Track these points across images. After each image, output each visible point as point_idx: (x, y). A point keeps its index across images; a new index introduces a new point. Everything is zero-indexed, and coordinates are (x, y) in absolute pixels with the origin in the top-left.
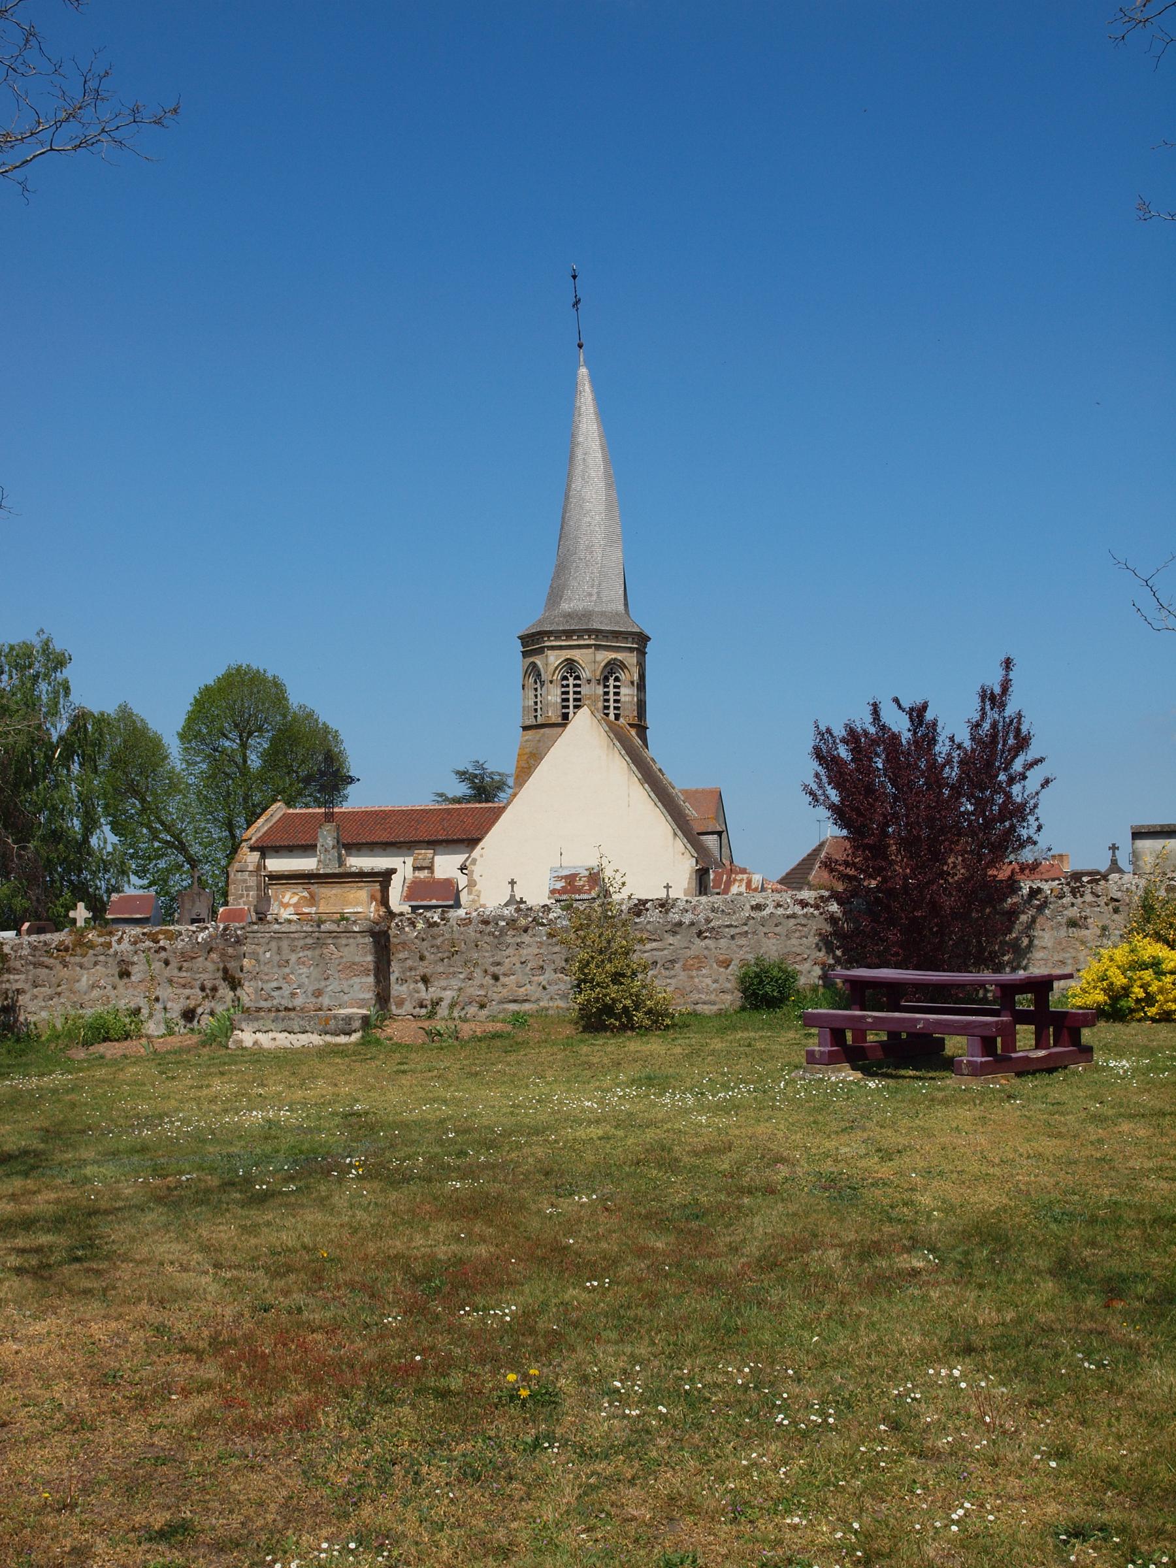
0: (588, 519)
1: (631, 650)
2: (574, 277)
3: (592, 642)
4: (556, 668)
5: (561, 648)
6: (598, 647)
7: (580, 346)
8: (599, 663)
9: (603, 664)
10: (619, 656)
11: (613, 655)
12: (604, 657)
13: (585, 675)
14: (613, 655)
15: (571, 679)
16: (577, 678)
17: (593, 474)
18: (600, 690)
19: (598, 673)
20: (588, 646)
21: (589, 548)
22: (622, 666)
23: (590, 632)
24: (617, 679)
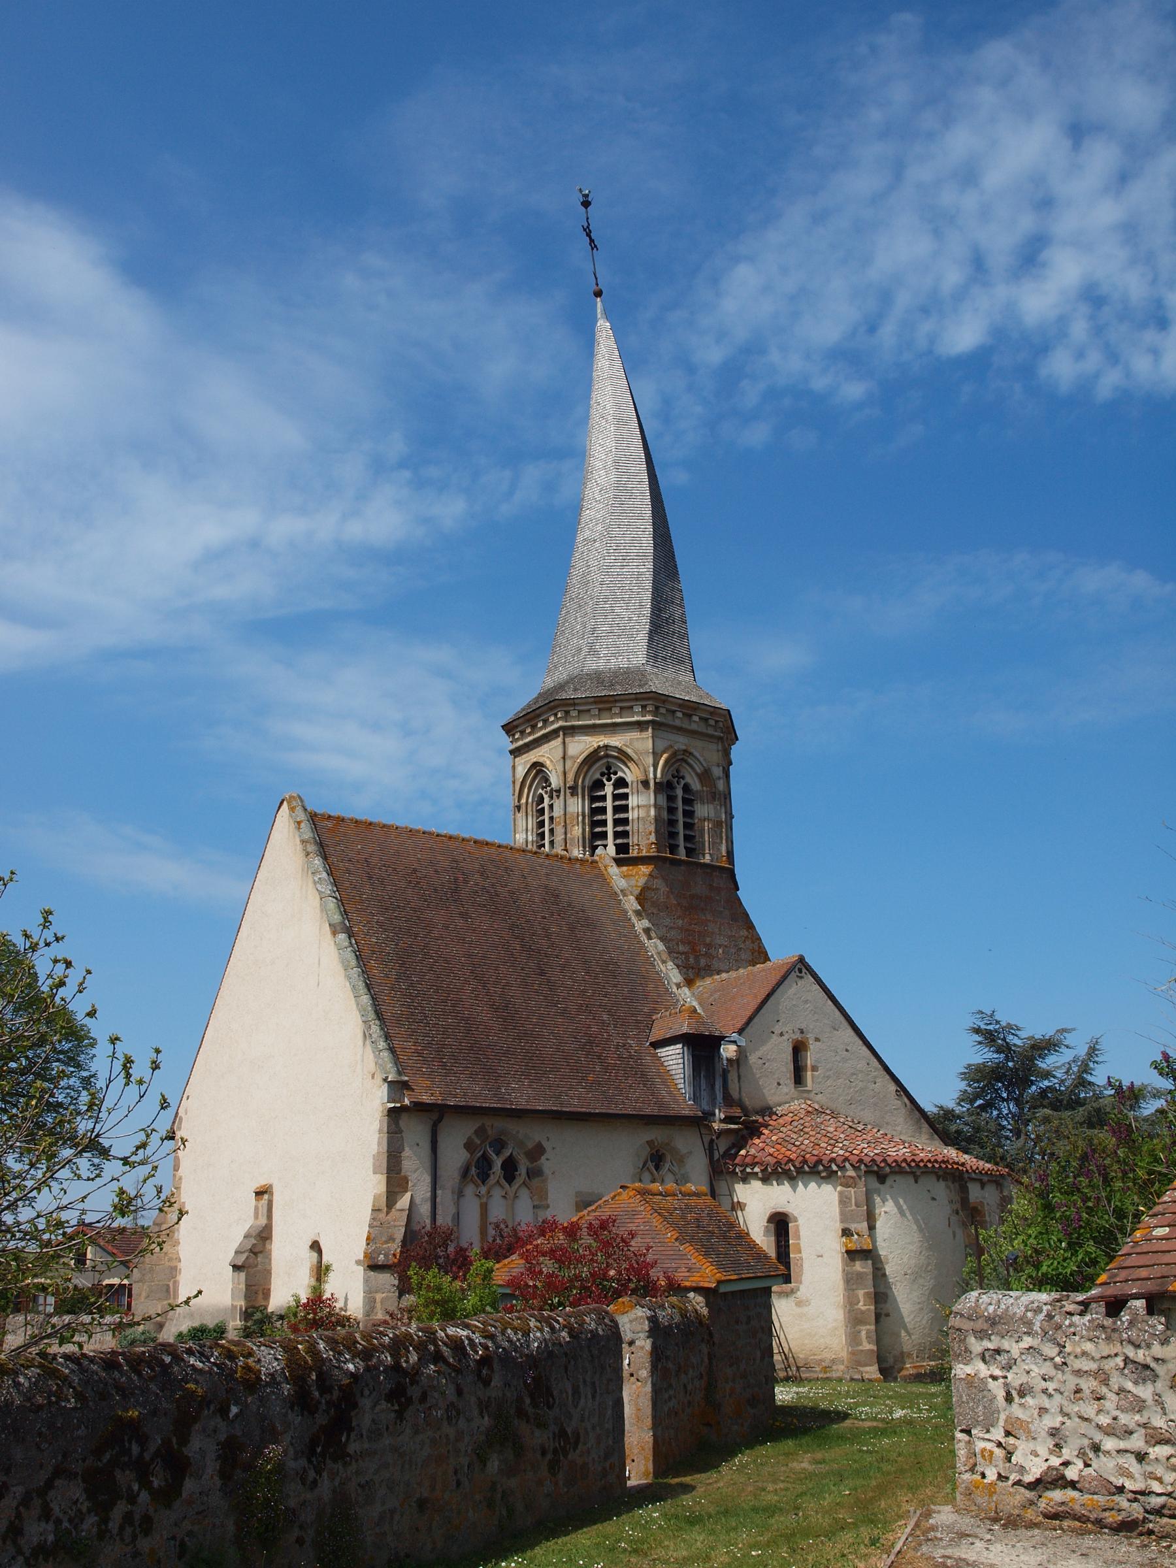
0: (587, 533)
1: (640, 726)
2: (586, 204)
7: (598, 294)
8: (574, 758)
10: (615, 741)
12: (581, 746)
13: (555, 781)
17: (598, 464)
18: (577, 805)
20: (555, 733)
22: (624, 756)
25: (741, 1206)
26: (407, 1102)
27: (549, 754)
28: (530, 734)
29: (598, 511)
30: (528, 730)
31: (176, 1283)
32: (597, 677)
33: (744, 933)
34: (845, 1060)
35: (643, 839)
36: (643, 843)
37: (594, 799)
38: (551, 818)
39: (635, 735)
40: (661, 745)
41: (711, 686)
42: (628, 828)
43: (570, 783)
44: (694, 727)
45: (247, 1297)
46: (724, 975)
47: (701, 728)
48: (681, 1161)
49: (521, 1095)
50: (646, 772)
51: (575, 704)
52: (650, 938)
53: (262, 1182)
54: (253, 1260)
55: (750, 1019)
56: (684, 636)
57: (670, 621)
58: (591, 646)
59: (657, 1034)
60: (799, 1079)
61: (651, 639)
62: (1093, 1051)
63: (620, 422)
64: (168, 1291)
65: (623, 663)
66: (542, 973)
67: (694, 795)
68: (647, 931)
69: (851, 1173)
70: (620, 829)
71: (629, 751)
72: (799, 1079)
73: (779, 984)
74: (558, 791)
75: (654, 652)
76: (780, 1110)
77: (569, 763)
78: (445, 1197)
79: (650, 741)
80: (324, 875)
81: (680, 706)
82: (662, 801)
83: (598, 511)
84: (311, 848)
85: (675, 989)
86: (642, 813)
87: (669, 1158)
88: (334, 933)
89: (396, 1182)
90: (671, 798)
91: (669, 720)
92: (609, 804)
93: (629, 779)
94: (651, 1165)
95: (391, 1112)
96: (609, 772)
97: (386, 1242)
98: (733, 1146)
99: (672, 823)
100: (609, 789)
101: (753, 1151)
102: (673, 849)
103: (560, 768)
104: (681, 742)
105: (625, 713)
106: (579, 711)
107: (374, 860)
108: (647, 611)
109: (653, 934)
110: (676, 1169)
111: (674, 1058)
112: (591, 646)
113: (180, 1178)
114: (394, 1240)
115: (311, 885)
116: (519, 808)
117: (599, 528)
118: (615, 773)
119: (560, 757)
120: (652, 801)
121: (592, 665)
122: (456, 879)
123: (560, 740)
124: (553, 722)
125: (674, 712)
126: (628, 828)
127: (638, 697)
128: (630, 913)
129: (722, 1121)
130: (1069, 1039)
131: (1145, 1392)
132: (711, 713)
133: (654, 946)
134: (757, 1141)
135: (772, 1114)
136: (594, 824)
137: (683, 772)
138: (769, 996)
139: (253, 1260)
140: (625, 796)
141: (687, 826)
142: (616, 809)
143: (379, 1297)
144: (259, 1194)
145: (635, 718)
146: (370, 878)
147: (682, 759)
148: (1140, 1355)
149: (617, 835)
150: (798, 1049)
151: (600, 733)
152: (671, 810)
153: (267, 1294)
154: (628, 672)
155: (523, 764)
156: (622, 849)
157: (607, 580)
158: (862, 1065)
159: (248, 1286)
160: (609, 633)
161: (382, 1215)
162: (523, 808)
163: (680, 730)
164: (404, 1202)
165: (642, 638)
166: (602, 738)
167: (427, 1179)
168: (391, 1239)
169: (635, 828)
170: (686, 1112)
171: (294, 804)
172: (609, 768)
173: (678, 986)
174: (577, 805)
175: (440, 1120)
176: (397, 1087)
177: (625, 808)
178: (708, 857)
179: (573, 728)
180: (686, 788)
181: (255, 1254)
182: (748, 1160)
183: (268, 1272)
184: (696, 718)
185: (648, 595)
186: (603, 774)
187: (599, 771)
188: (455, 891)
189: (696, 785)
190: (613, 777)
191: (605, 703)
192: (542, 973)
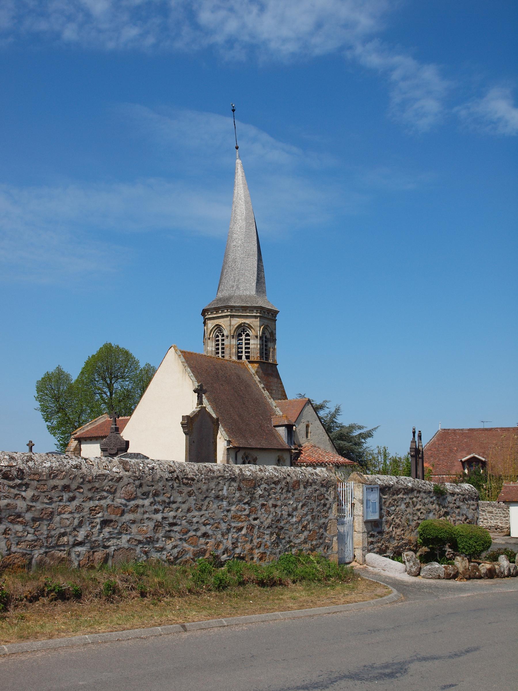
0: (235, 243)
1: (256, 317)
2: (233, 110)
3: (229, 313)
4: (211, 330)
5: (214, 318)
6: (232, 316)
7: (237, 148)
9: (236, 326)
10: (247, 321)
12: (237, 322)
13: (226, 333)
15: (220, 336)
16: (223, 336)
17: (239, 218)
18: (234, 342)
19: (232, 332)
20: (227, 316)
21: (234, 261)
22: (250, 327)
23: (227, 307)
24: (248, 335)
26: (231, 446)
27: (223, 323)
28: (215, 314)
32: (240, 297)
33: (280, 385)
34: (317, 430)
35: (255, 355)
38: (223, 344)
39: (254, 320)
40: (262, 323)
44: (270, 317)
49: (253, 444)
56: (264, 283)
58: (237, 286)
59: (274, 422)
61: (257, 285)
62: (337, 410)
63: (246, 202)
65: (248, 293)
67: (268, 339)
68: (263, 388)
69: (331, 466)
70: (247, 350)
71: (252, 325)
72: (307, 437)
74: (227, 337)
75: (257, 291)
76: (303, 445)
77: (232, 327)
84: (186, 364)
90: (262, 341)
93: (251, 334)
95: (228, 449)
96: (244, 331)
98: (296, 457)
101: (302, 459)
103: (228, 328)
107: (197, 367)
111: (282, 431)
112: (237, 286)
119: (229, 325)
120: (259, 343)
121: (238, 293)
123: (229, 319)
131: (484, 514)
133: (266, 393)
135: (302, 446)
136: (238, 348)
140: (249, 340)
141: (266, 350)
145: (254, 314)
148: (483, 509)
149: (246, 352)
150: (307, 426)
155: (211, 324)
156: (247, 357)
158: (321, 431)
162: (211, 339)
165: (254, 284)
170: (287, 447)
172: (244, 330)
175: (239, 451)
176: (229, 442)
177: (249, 344)
179: (234, 315)
180: (266, 337)
185: (256, 269)
186: (242, 332)
189: (268, 336)
190: (245, 333)
191: (244, 308)
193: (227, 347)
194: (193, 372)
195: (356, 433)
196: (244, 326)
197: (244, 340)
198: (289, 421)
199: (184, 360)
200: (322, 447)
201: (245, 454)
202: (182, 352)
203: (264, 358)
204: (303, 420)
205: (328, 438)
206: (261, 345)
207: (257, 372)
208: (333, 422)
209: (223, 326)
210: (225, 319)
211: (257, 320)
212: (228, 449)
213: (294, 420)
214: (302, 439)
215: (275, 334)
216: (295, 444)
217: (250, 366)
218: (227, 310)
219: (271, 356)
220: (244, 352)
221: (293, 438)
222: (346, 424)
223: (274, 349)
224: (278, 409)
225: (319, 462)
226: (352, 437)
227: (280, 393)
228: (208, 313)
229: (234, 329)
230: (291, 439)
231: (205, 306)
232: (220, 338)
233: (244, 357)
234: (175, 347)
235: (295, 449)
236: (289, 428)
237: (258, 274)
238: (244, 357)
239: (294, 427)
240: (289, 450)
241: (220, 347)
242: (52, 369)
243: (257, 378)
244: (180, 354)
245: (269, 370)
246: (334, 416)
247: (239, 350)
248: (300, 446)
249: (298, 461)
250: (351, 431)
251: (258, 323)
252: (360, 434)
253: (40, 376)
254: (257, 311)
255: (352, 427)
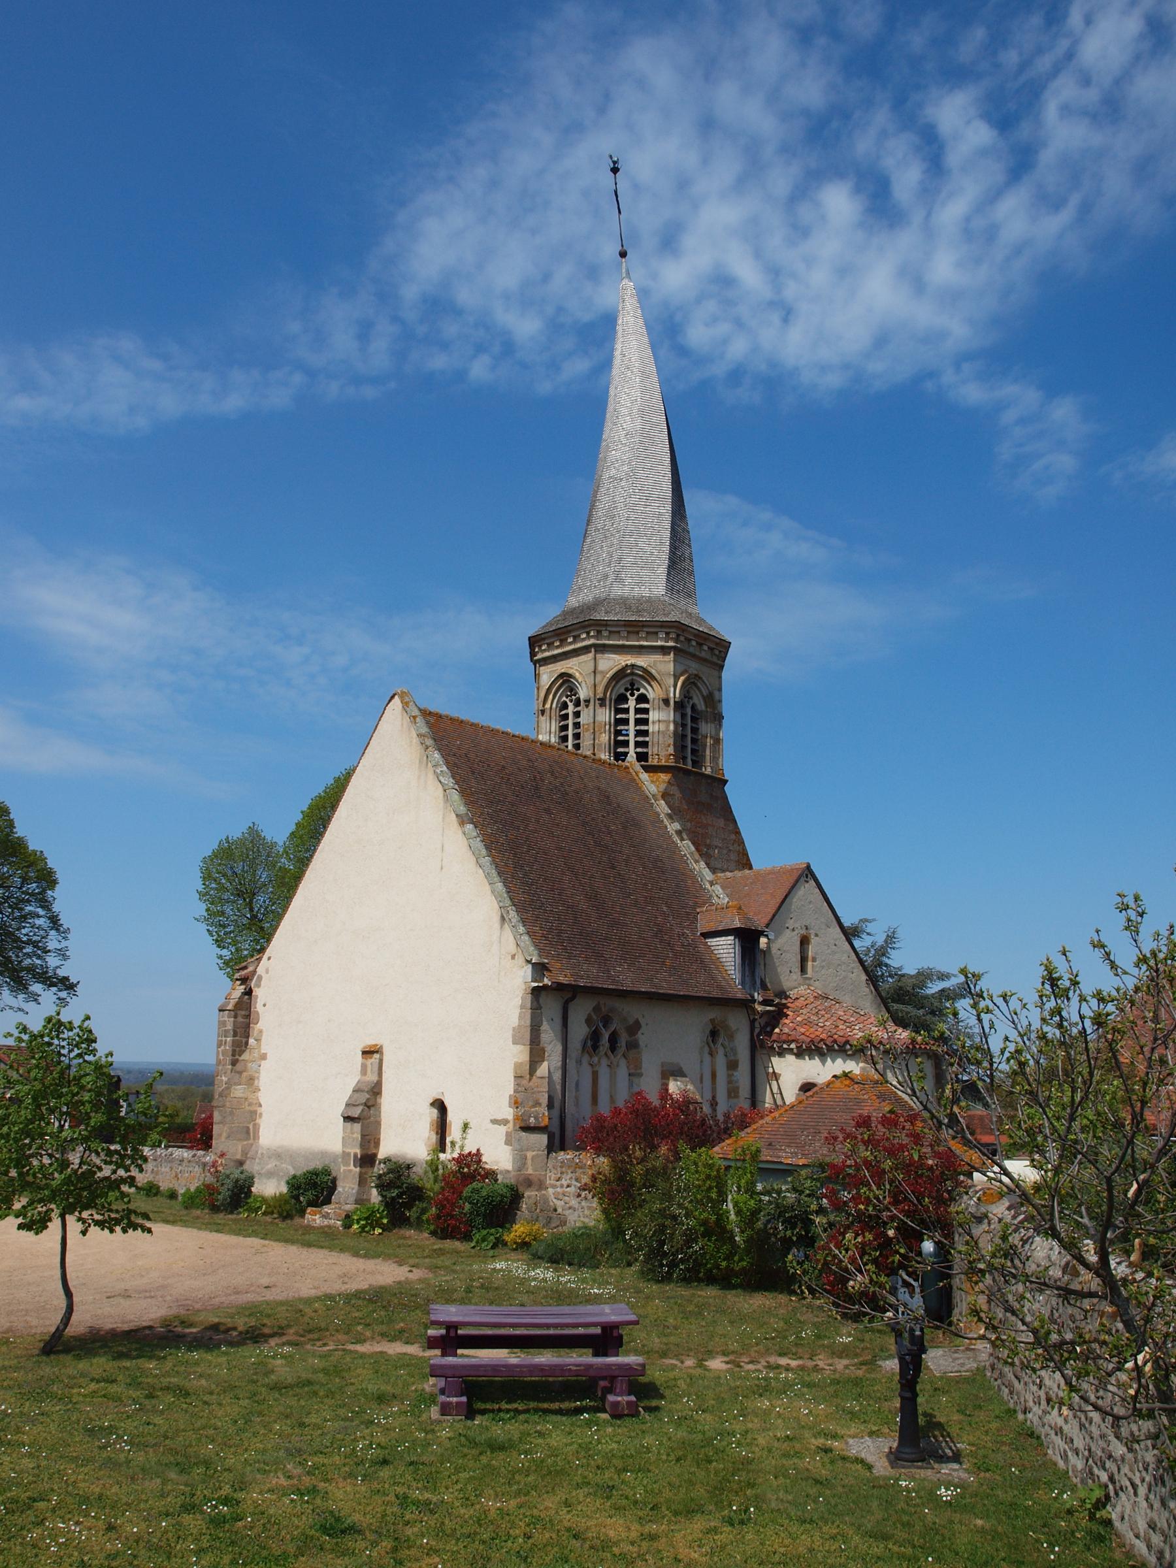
0: (613, 472)
1: (664, 650)
3: (592, 641)
6: (601, 649)
8: (604, 673)
9: (609, 675)
10: (641, 661)
11: (629, 660)
12: (611, 663)
13: (583, 694)
14: (629, 660)
17: (624, 411)
19: (600, 689)
22: (648, 676)
24: (643, 699)
25: (776, 1076)
26: (546, 981)
27: (578, 667)
28: (557, 647)
29: (624, 453)
30: (557, 643)
31: (257, 1128)
32: (624, 602)
33: (733, 837)
34: (834, 953)
35: (662, 749)
36: (663, 753)
37: (618, 711)
38: (577, 725)
39: (658, 657)
40: (681, 668)
41: (717, 621)
42: (647, 739)
43: (600, 695)
44: (703, 655)
45: (362, 1146)
46: (729, 874)
47: (708, 657)
48: (731, 1037)
49: (627, 979)
50: (667, 692)
51: (606, 625)
52: (682, 840)
53: (370, 1041)
54: (364, 1113)
55: (774, 916)
56: (691, 573)
57: (682, 558)
59: (703, 925)
60: (803, 970)
61: (669, 574)
62: (891, 939)
63: (644, 375)
64: (248, 1132)
66: (613, 868)
67: (698, 713)
68: (679, 833)
70: (640, 739)
71: (653, 672)
72: (803, 970)
73: (793, 887)
74: (587, 701)
75: (671, 586)
76: (792, 994)
77: (599, 677)
78: (571, 1064)
79: (672, 664)
80: (445, 768)
81: (695, 635)
82: (679, 720)
83: (624, 453)
84: (429, 742)
85: (708, 886)
86: (663, 727)
87: (722, 1033)
88: (462, 823)
89: (536, 1055)
90: (683, 716)
91: (685, 647)
92: (632, 716)
93: (651, 695)
94: (710, 1039)
96: (632, 688)
97: (534, 1106)
98: (767, 1024)
99: (684, 736)
100: (632, 703)
101: (786, 1030)
102: (684, 758)
103: (590, 681)
104: (694, 667)
105: (631, 636)
106: (610, 632)
107: (472, 756)
108: (666, 549)
109: (685, 837)
110: (726, 1043)
111: (726, 949)
113: (261, 1031)
114: (540, 1104)
115: (431, 776)
116: (543, 712)
117: (625, 468)
118: (638, 690)
119: (590, 671)
120: (672, 718)
121: (618, 591)
122: (535, 777)
123: (591, 655)
124: (584, 639)
125: (690, 640)
126: (647, 739)
127: (663, 625)
128: (662, 816)
129: (761, 1003)
130: (870, 928)
132: (717, 644)
133: (686, 847)
134: (787, 1021)
135: (787, 997)
136: (618, 733)
137: (692, 693)
138: (786, 896)
139: (364, 1113)
140: (646, 711)
141: (694, 741)
142: (638, 722)
143: (530, 1154)
144: (367, 1053)
145: (659, 643)
146: (473, 773)
147: (693, 683)
149: (637, 744)
150: (804, 941)
151: (627, 653)
152: (684, 725)
153: (377, 1144)
154: (649, 600)
155: (547, 675)
156: (642, 757)
157: (633, 516)
158: (844, 958)
159: (363, 1136)
160: (628, 563)
161: (524, 1082)
163: (693, 656)
164: (543, 1069)
165: (662, 570)
166: (629, 657)
167: (559, 1048)
168: (537, 1104)
169: (656, 740)
170: (739, 996)
171: (407, 699)
172: (632, 684)
173: (712, 884)
174: (605, 715)
176: (540, 969)
177: (645, 722)
178: (709, 769)
179: (604, 646)
180: (693, 707)
181: (369, 1107)
182: (784, 1037)
183: (378, 1123)
184: (706, 648)
185: (667, 534)
186: (627, 690)
187: (624, 688)
188: (537, 788)
189: (701, 706)
191: (634, 628)
192: (613, 868)
193: (587, 730)
194: (447, 763)
195: (934, 988)
196: (632, 674)
197: (632, 711)
198: (745, 918)
199: (425, 730)
200: (847, 1000)
201: (597, 1009)
202: (426, 713)
203: (689, 762)
204: (790, 924)
205: (864, 977)
206: (681, 724)
207: (665, 796)
208: (881, 964)
209: (577, 675)
210: (583, 658)
211: (667, 658)
212: (534, 989)
213: (765, 920)
214: (788, 977)
215: (720, 701)
216: (764, 987)
217: (644, 776)
218: (588, 633)
219: (708, 758)
220: (632, 744)
221: (760, 972)
222: (910, 970)
223: (717, 741)
224: (718, 889)
225: (835, 1041)
226: (926, 997)
227: (733, 857)
228: (540, 646)
229: (605, 681)
230: (753, 973)
231: (534, 627)
232: (571, 709)
233: (632, 756)
234: (402, 695)
235: (765, 1002)
236: (748, 938)
237: (674, 548)
238: (632, 756)
239: (763, 940)
240: (746, 1004)
241: (570, 733)
242: (237, 831)
243: (662, 807)
244: (416, 712)
245: (701, 792)
246: (882, 951)
247: (620, 738)
248: (782, 994)
249: (774, 1037)
250: (923, 985)
251: (671, 667)
252: (943, 990)
253: (209, 847)
254: (667, 634)
255: (925, 976)
